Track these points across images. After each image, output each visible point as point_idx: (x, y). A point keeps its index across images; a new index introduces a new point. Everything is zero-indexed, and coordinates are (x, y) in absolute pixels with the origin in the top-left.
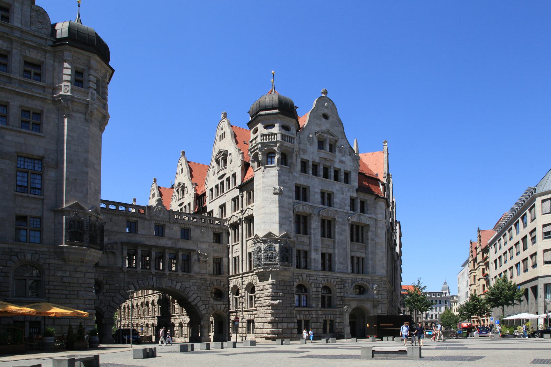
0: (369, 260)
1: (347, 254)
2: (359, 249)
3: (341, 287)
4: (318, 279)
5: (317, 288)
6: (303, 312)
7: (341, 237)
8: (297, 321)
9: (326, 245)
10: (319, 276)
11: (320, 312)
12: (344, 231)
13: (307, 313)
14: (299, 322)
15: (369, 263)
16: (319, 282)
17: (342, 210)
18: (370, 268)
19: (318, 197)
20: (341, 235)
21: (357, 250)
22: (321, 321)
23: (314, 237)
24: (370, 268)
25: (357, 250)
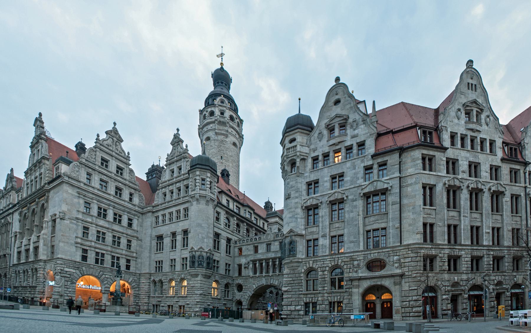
0: (389, 229)
1: (359, 230)
2: (378, 220)
3: (350, 266)
4: (325, 262)
5: (323, 271)
6: (309, 296)
7: (351, 215)
8: (303, 304)
9: (336, 228)
10: (325, 260)
11: (326, 295)
12: (356, 207)
13: (313, 296)
14: (307, 305)
15: (390, 233)
16: (325, 265)
17: (352, 186)
18: (391, 238)
19: (328, 185)
20: (352, 212)
21: (374, 222)
22: (327, 303)
23: (322, 224)
24: (391, 238)
25: (374, 222)
